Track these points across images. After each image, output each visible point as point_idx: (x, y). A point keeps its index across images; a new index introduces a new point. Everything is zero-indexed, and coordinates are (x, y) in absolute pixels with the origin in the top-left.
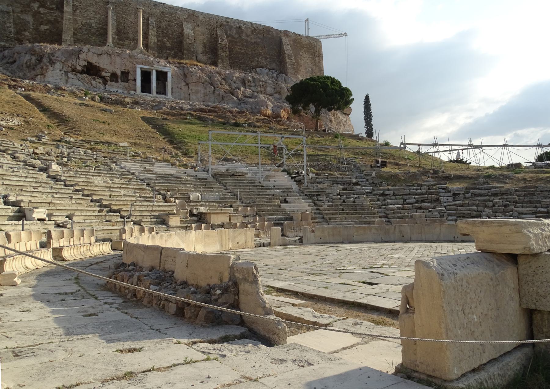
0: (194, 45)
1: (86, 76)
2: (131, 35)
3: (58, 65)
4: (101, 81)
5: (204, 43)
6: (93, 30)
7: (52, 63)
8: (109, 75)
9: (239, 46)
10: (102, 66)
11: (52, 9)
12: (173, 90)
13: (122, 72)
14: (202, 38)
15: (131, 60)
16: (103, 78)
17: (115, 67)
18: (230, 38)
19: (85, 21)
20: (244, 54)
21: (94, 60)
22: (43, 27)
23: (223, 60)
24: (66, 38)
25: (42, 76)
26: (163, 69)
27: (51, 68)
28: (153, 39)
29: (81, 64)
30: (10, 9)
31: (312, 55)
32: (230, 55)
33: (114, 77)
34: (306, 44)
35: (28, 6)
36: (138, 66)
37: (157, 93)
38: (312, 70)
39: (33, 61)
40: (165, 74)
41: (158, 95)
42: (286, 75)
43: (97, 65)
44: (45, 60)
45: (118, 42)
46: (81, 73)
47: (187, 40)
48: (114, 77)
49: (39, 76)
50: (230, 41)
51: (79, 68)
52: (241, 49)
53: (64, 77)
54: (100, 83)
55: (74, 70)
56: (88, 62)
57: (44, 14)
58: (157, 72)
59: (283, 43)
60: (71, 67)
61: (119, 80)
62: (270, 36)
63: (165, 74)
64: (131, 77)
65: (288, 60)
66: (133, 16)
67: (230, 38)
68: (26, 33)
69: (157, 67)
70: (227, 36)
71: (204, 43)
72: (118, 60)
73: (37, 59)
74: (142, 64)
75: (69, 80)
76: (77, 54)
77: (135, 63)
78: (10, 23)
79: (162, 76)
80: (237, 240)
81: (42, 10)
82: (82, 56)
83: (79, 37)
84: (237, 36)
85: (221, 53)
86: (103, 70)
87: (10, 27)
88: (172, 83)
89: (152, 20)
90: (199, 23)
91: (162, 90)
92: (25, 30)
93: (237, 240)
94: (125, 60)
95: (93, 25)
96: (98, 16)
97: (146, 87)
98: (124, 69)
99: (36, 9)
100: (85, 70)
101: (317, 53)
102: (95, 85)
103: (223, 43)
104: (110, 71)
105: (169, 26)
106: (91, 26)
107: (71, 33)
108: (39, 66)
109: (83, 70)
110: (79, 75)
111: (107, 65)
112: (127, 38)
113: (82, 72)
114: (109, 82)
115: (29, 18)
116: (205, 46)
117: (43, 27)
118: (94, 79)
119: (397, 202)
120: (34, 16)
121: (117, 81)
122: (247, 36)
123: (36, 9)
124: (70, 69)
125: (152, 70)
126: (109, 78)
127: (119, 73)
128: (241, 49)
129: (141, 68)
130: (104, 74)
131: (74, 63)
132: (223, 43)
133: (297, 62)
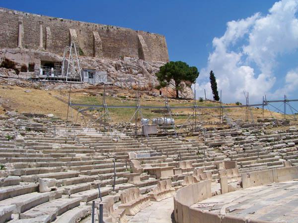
1: (5, 68)
4: (14, 72)
6: (7, 38)
8: (20, 67)
10: (15, 61)
13: (30, 65)
21: (11, 57)
28: (49, 42)
32: (103, 49)
33: (24, 69)
38: (161, 56)
42: (144, 60)
50: (102, 40)
54: (14, 73)
59: (140, 39)
65: (144, 50)
67: (102, 38)
70: (101, 36)
72: (27, 57)
80: (202, 192)
85: (97, 48)
86: (17, 64)
93: (202, 192)
95: (8, 34)
96: (11, 28)
98: (31, 62)
104: (21, 64)
111: (20, 60)
114: (20, 72)
116: (85, 44)
119: (282, 146)
121: (26, 72)
122: (114, 35)
127: (28, 66)
130: (17, 67)
133: (150, 51)
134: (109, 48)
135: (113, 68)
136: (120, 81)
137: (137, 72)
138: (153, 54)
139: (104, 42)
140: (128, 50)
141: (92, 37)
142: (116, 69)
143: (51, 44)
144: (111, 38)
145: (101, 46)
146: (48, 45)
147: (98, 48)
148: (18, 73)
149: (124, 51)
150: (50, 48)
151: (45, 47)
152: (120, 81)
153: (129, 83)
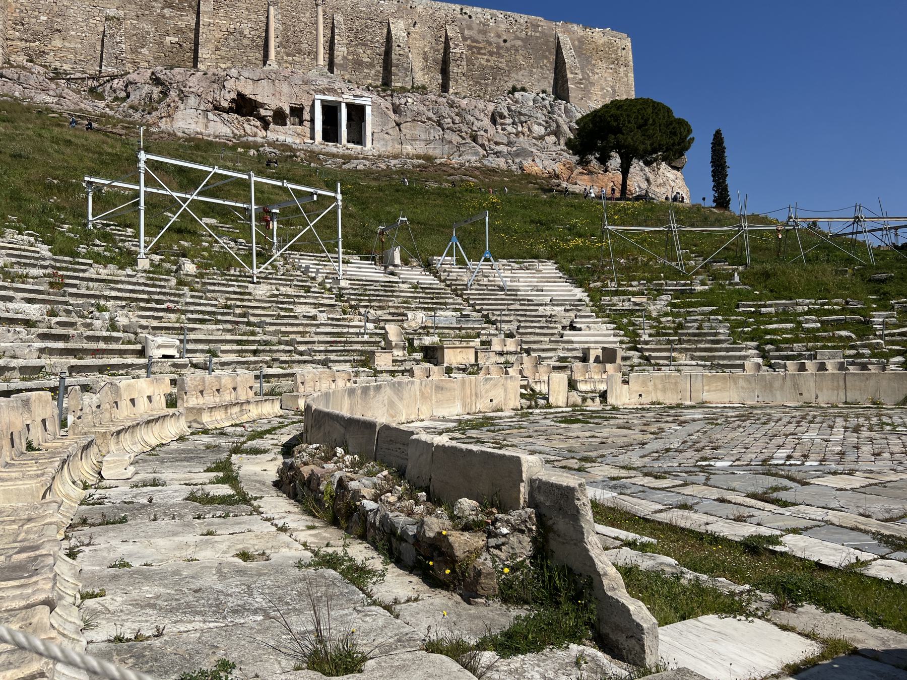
0: (408, 57)
1: (236, 116)
2: (305, 47)
3: (192, 101)
4: (258, 123)
5: (425, 53)
7: (183, 97)
8: (270, 113)
9: (484, 54)
10: (259, 99)
11: (183, 9)
12: (375, 135)
13: (291, 108)
14: (420, 44)
15: (306, 87)
16: (262, 119)
17: (280, 100)
18: (469, 42)
19: (233, 27)
20: (492, 68)
21: (248, 90)
22: (169, 39)
23: (457, 81)
24: (204, 56)
25: (168, 119)
26: (358, 101)
27: (182, 107)
28: (341, 51)
29: (226, 99)
30: (121, 13)
31: (613, 63)
33: (279, 117)
34: (603, 45)
35: (149, 8)
36: (317, 97)
37: (348, 142)
38: (614, 91)
39: (155, 96)
40: (362, 108)
41: (350, 145)
42: (568, 101)
43: (253, 97)
44: (173, 94)
45: (285, 58)
46: (228, 113)
47: (397, 48)
48: (279, 117)
49: (164, 119)
51: (225, 104)
52: (488, 61)
53: (201, 120)
54: (257, 127)
55: (217, 108)
56: (240, 95)
57: (170, 18)
58: (348, 105)
60: (212, 103)
61: (288, 122)
62: (538, 34)
63: (362, 108)
64: (306, 116)
65: (569, 76)
66: (308, 14)
68: (144, 51)
69: (348, 98)
70: (465, 39)
71: (425, 53)
72: (285, 88)
73: (161, 92)
74: (324, 94)
75: (209, 125)
76: (220, 82)
77: (312, 92)
78: (121, 35)
79: (357, 113)
81: (167, 11)
82: (229, 84)
83: (223, 53)
84: (480, 37)
85: (453, 69)
86: (262, 105)
87: (121, 43)
88: (373, 124)
89: (339, 18)
90: (416, 19)
91: (357, 136)
92: (143, 46)
94: (296, 88)
95: (246, 32)
97: (331, 134)
99: (159, 11)
100: (234, 105)
101: (623, 59)
102: (249, 131)
103: (457, 50)
104: (274, 107)
105: (366, 27)
106: (241, 33)
107: (211, 46)
108: (163, 105)
109: (230, 108)
110: (225, 115)
112: (300, 52)
113: (228, 111)
114: (272, 126)
115: (147, 27)
116: (426, 59)
117: (169, 39)
118: (248, 120)
120: (155, 23)
121: (285, 124)
122: (499, 36)
123: (159, 11)
124: (211, 106)
125: (340, 102)
126: (271, 119)
127: (288, 111)
128: (488, 61)
129: (322, 101)
130: (263, 112)
131: (217, 96)
132: (457, 50)
133: (586, 78)
134: (483, 68)
135: (487, 122)
136: (498, 154)
137: (542, 131)
138: (593, 84)
139: (473, 53)
140: (531, 74)
141: (443, 39)
142: (494, 121)
143: (344, 58)
144: (490, 44)
145: (464, 63)
146: (338, 60)
147: (455, 70)
148: (266, 126)
149: (520, 78)
150: (343, 67)
151: (331, 66)
152: (498, 154)
153: (517, 160)
